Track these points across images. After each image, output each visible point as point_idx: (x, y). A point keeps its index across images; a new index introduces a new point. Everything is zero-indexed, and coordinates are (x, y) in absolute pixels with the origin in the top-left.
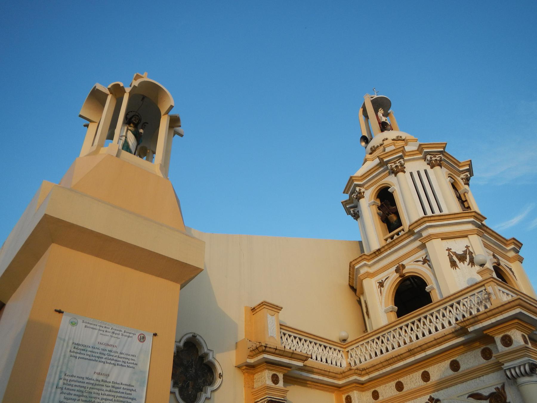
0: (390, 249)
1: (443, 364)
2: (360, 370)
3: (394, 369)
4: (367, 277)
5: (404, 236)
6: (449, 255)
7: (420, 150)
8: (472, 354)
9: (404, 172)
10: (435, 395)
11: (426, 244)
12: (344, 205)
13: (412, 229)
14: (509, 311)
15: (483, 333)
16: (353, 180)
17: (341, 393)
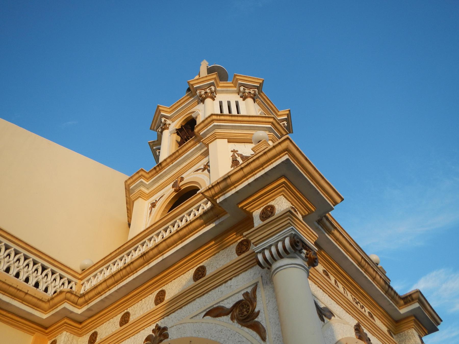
0: (173, 163)
2: (75, 295)
4: (139, 197)
6: (233, 156)
7: (234, 82)
9: (214, 100)
10: (161, 324)
16: (160, 110)
17: (47, 337)
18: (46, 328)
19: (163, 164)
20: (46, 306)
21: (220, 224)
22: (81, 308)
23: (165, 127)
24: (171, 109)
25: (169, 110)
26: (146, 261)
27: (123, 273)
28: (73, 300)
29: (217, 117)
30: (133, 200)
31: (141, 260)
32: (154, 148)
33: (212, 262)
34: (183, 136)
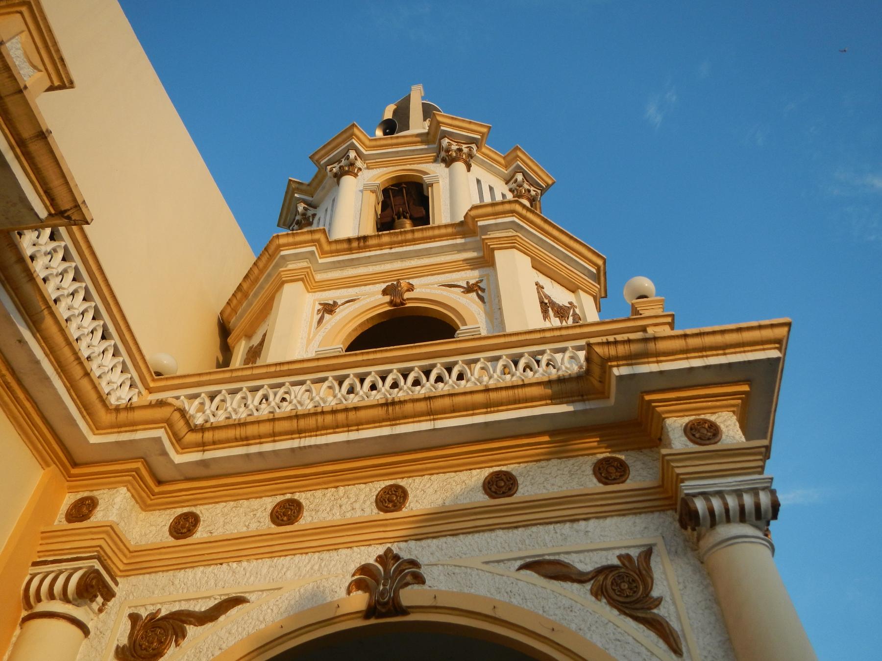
0: (391, 248)
1: (464, 476)
2: (187, 423)
3: (305, 447)
4: (302, 280)
5: (443, 231)
7: (509, 158)
8: (563, 466)
10: (405, 551)
11: (497, 253)
12: (290, 192)
13: (474, 218)
14: (748, 351)
15: (643, 397)
18: (75, 465)
19: (370, 240)
20: (105, 417)
21: (584, 412)
22: (182, 453)
23: (351, 170)
24: (374, 143)
25: (367, 143)
26: (391, 416)
27: (325, 421)
28: (179, 430)
29: (523, 210)
30: (284, 279)
31: (380, 412)
32: (296, 195)
33: (531, 473)
34: (395, 205)
